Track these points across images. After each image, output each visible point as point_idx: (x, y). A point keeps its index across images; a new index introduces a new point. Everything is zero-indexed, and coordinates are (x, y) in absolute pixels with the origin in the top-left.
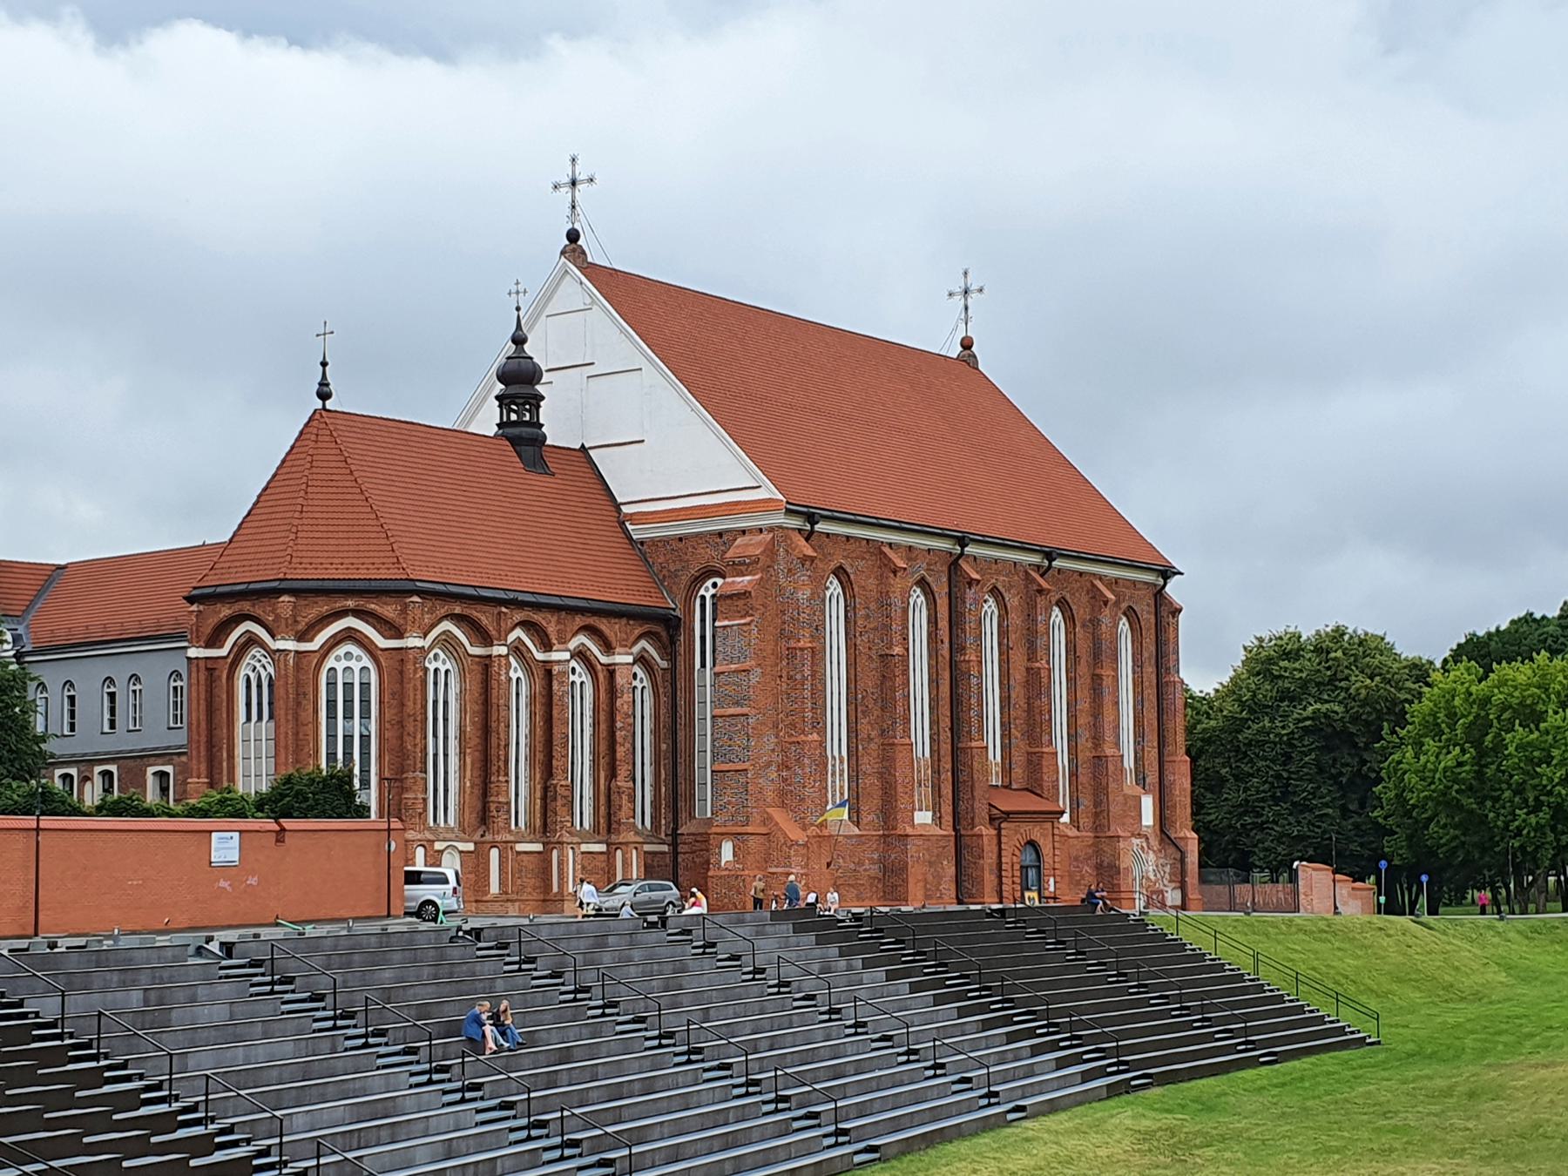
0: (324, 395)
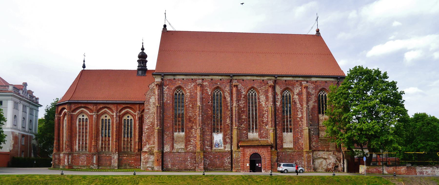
0: (84, 66)
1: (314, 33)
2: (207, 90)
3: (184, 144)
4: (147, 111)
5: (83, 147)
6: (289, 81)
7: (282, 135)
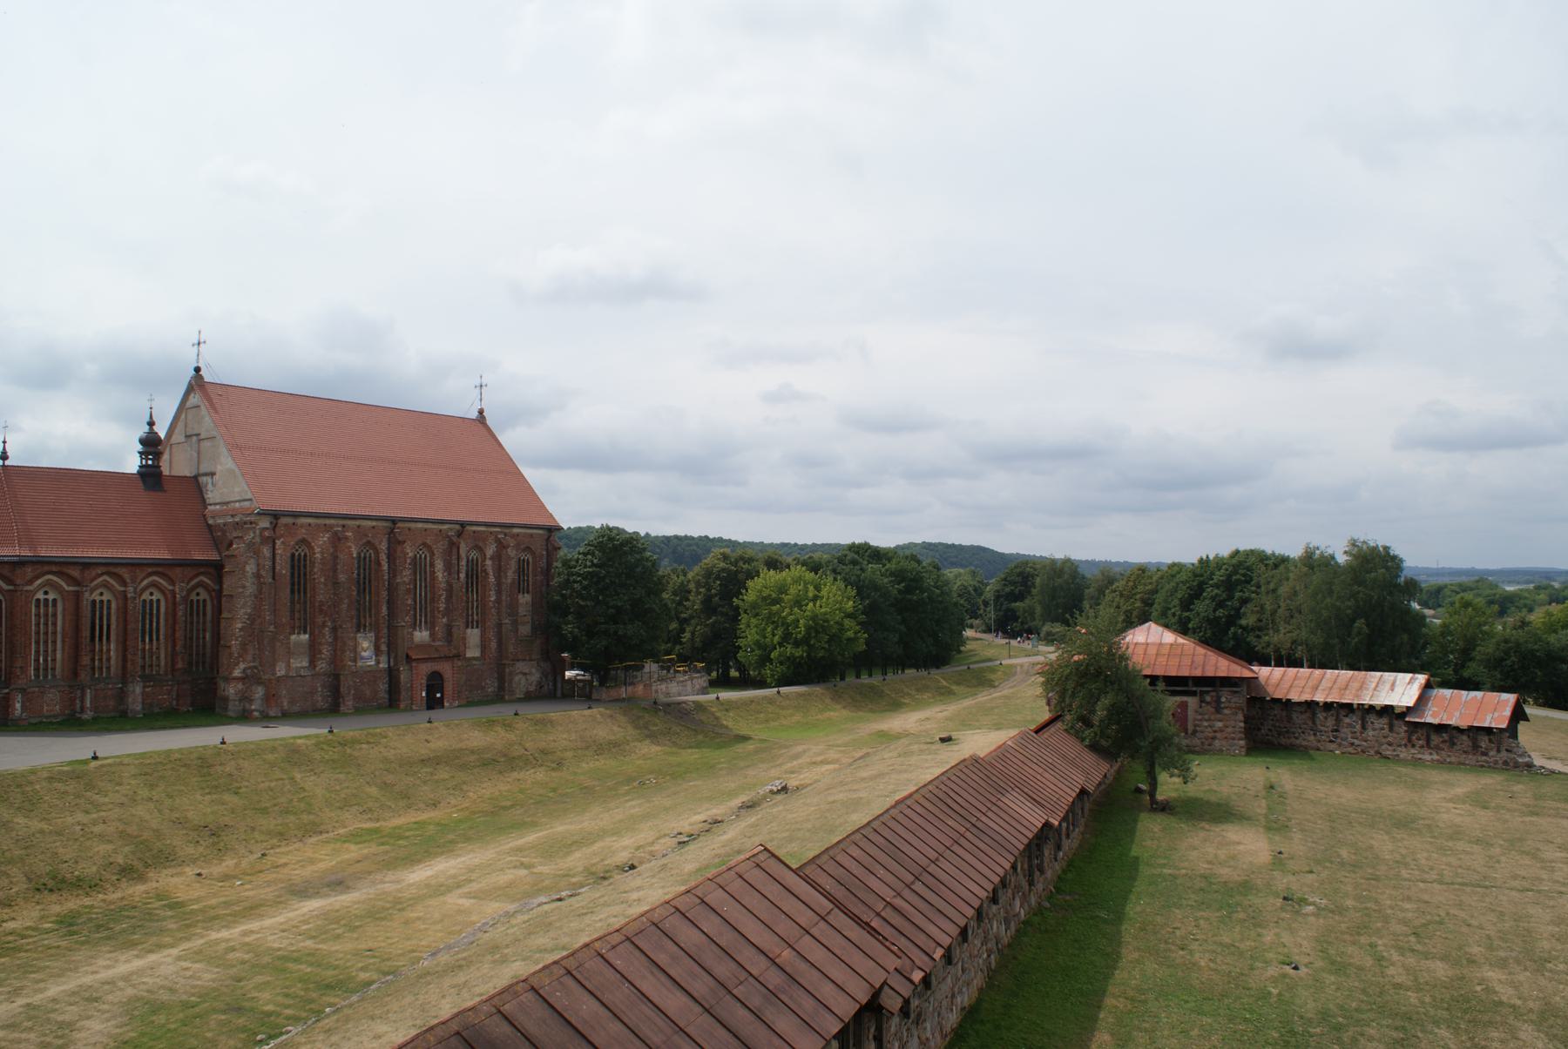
1: (474, 415)
2: (350, 547)
3: (307, 659)
4: (241, 590)
5: (46, 669)
6: (478, 532)
7: (465, 633)
